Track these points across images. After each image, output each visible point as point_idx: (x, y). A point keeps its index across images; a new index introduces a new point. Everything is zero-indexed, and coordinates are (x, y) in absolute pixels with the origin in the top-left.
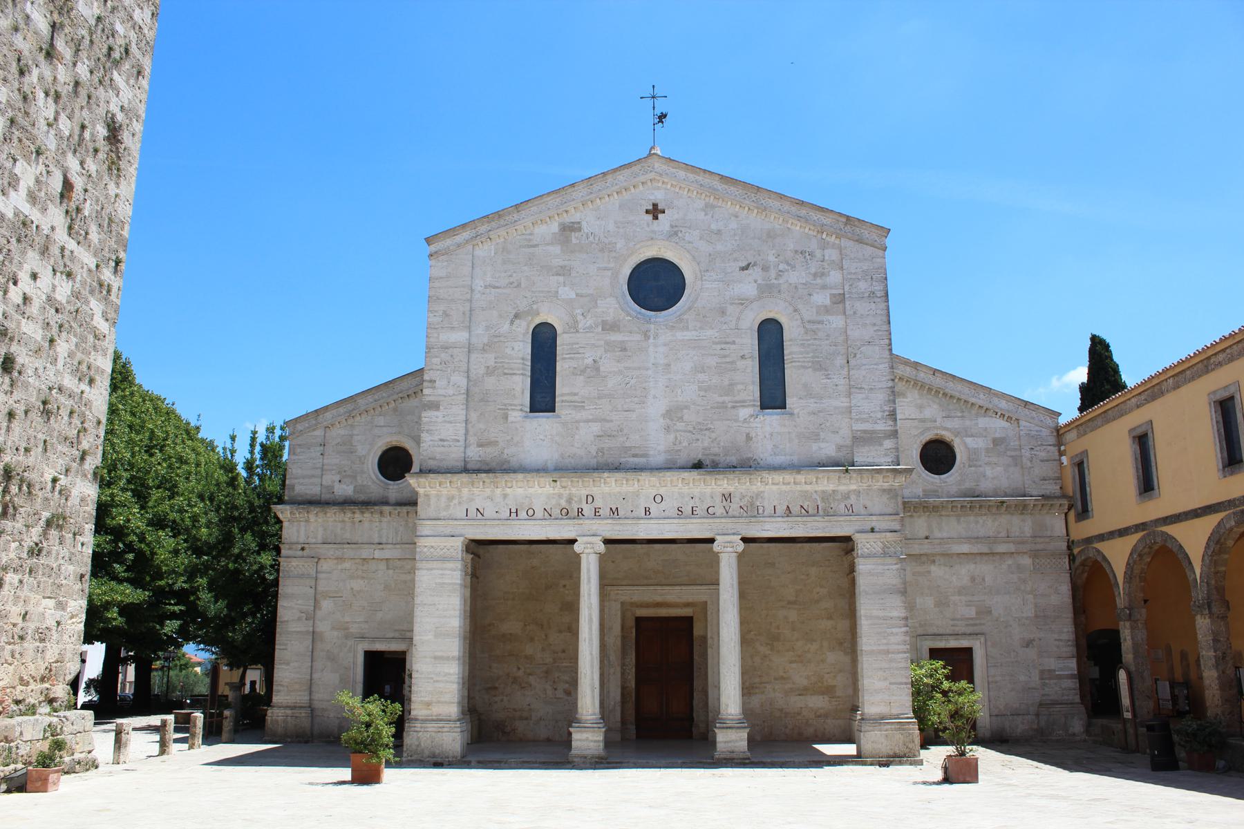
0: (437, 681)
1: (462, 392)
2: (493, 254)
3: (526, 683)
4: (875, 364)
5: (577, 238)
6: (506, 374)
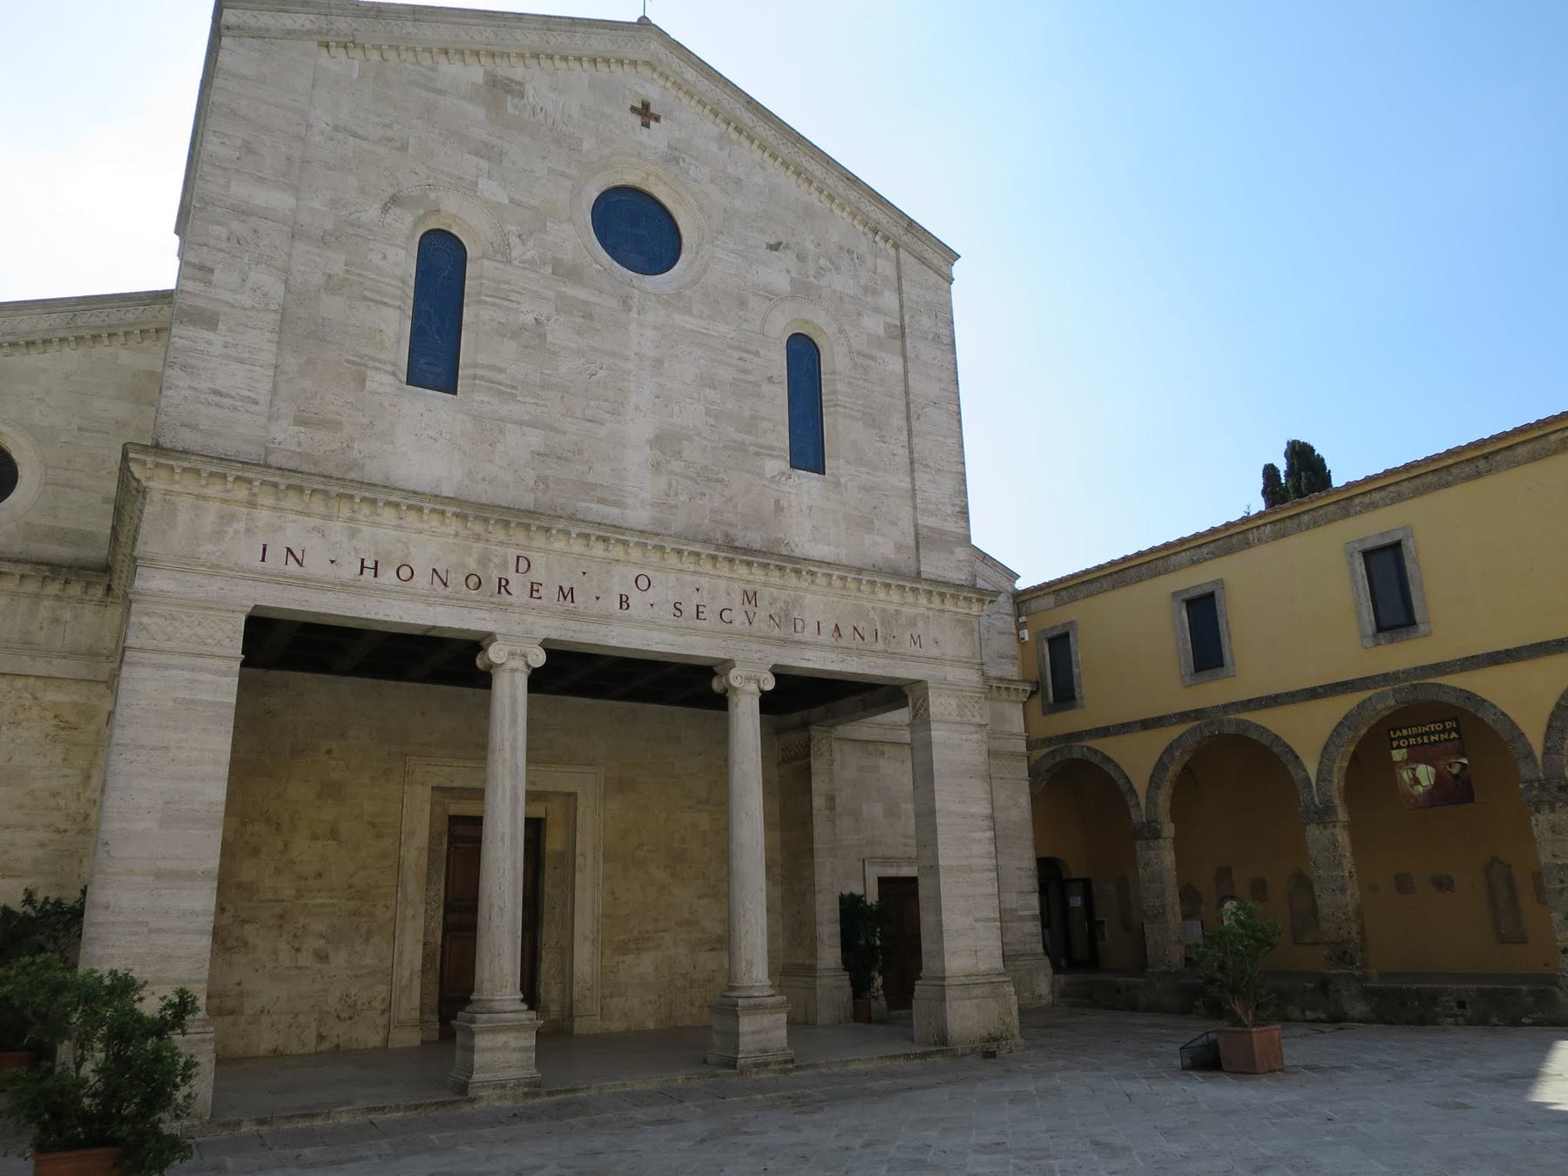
0: (160, 931)
1: (272, 307)
2: (355, 76)
3: (237, 939)
4: (945, 437)
5: (516, 107)
6: (366, 298)
